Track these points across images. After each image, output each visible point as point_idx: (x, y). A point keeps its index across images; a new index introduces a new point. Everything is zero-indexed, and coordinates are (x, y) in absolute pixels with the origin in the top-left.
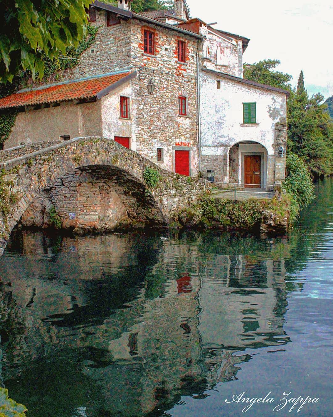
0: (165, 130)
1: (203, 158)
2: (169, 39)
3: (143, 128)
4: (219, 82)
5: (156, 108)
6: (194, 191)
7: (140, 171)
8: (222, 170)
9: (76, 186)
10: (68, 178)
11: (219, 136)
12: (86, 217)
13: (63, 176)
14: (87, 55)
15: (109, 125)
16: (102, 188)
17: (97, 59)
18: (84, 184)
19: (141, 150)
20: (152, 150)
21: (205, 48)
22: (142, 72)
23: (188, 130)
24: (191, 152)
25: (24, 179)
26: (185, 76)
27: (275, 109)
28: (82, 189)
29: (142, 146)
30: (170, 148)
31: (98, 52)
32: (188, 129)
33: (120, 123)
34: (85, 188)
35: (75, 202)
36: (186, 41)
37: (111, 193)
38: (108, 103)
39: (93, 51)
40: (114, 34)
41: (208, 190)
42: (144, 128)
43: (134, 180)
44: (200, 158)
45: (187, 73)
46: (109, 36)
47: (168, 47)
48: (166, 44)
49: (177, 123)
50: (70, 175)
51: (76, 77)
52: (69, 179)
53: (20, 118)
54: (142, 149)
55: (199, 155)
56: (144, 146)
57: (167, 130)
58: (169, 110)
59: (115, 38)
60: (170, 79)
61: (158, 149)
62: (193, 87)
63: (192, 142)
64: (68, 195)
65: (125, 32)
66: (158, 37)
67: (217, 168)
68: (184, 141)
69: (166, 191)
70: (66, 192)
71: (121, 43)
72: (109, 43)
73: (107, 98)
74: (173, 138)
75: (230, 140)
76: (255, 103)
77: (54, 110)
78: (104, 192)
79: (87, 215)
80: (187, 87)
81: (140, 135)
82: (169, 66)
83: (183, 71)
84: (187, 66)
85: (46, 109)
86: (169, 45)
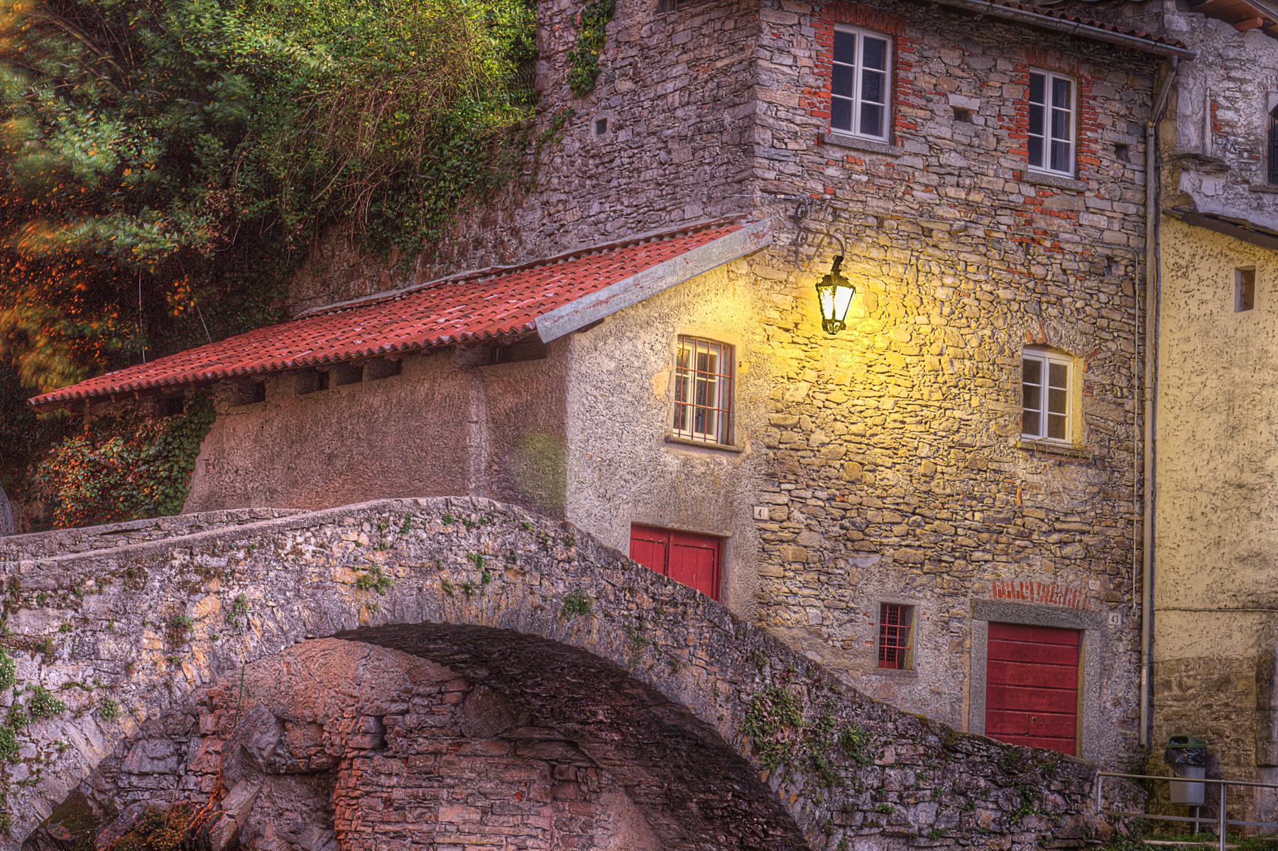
0: (927, 513)
1: (1160, 677)
2: (979, 64)
3: (803, 493)
4: (1247, 277)
8: (1249, 740)
9: (436, 753)
10: (407, 711)
11: (1242, 560)
13: (385, 706)
14: (578, 145)
15: (608, 466)
16: (561, 773)
17: (617, 162)
18: (478, 746)
19: (787, 605)
20: (849, 610)
21: (1190, 103)
22: (812, 226)
23: (1074, 523)
24: (1091, 644)
25: (101, 636)
26: (1067, 247)
28: (463, 770)
30: (961, 607)
31: (621, 128)
34: (479, 764)
35: (425, 827)
37: (605, 796)
38: (612, 365)
39: (602, 126)
40: (690, 46)
41: (1113, 819)
42: (808, 494)
43: (688, 727)
44: (1145, 672)
45: (1081, 232)
46: (671, 57)
47: (974, 104)
48: (958, 90)
50: (416, 700)
51: (529, 246)
52: (411, 720)
53: (240, 433)
55: (1140, 660)
56: (805, 585)
57: (945, 514)
58: (957, 414)
59: (691, 65)
61: (884, 605)
62: (1117, 301)
63: (1095, 585)
64: (398, 794)
65: (736, 36)
66: (913, 58)
67: (1224, 725)
68: (1047, 579)
71: (718, 86)
72: (670, 86)
73: (604, 339)
74: (978, 555)
77: (374, 398)
78: (570, 790)
80: (1079, 304)
82: (975, 197)
83: (1057, 221)
84: (1080, 193)
85: (345, 390)
86: (977, 96)
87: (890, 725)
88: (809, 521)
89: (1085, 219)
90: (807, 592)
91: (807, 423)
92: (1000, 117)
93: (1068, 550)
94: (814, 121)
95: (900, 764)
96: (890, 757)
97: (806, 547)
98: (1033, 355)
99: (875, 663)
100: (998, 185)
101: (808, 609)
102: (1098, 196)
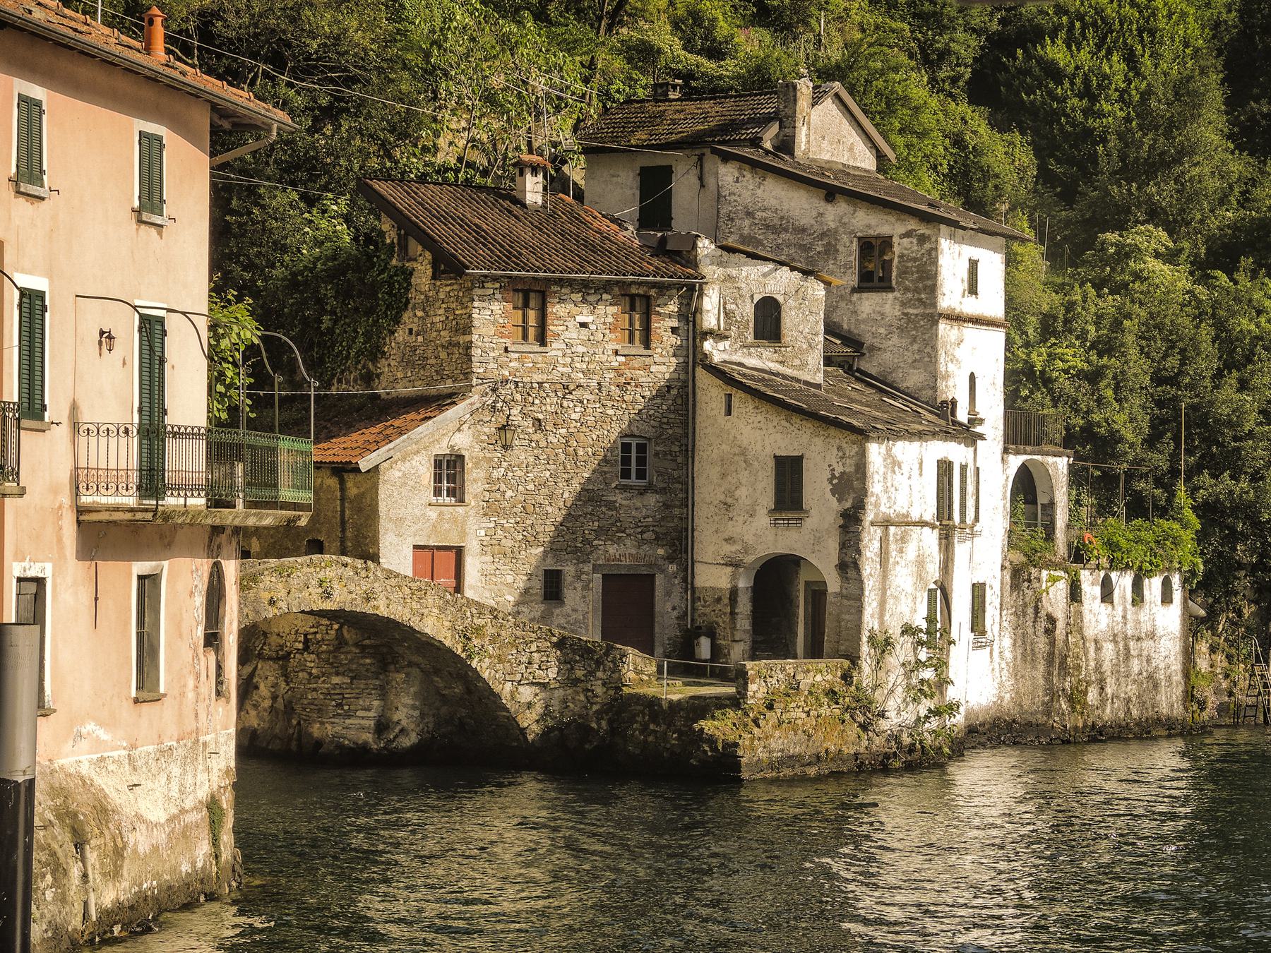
1: (697, 595)
5: (548, 474)
6: (599, 674)
12: (348, 721)
24: (659, 580)
27: (843, 473)
32: (651, 519)
33: (433, 514)
36: (653, 292)
38: (400, 474)
39: (411, 331)
46: (437, 305)
47: (589, 319)
49: (611, 505)
52: (319, 636)
54: (497, 572)
60: (591, 397)
62: (672, 408)
63: (661, 552)
67: (720, 620)
68: (633, 551)
70: (312, 665)
73: (396, 462)
74: (596, 542)
75: (746, 551)
76: (802, 457)
78: (392, 667)
79: (349, 717)
82: (592, 366)
89: (654, 368)
91: (503, 487)
92: (604, 323)
93: (645, 536)
94: (503, 340)
96: (534, 648)
98: (627, 440)
99: (541, 599)
100: (604, 358)
102: (661, 355)
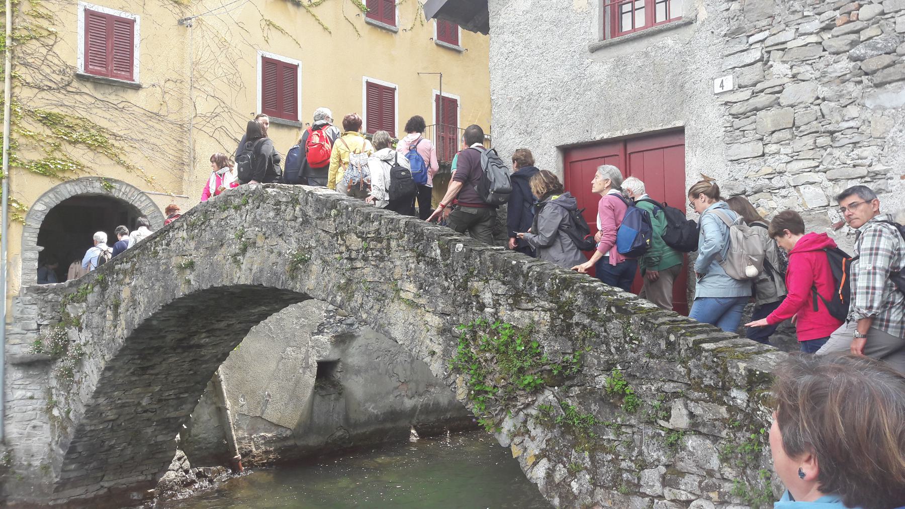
7: (435, 321)
19: (772, 191)
29: (775, 164)
42: (789, 34)
54: (776, 182)
56: (795, 157)
69: (666, 492)
81: (754, 94)
87: (680, 368)
88: (795, 70)
90: (796, 166)
95: (695, 427)
97: (792, 106)
101: (801, 188)
